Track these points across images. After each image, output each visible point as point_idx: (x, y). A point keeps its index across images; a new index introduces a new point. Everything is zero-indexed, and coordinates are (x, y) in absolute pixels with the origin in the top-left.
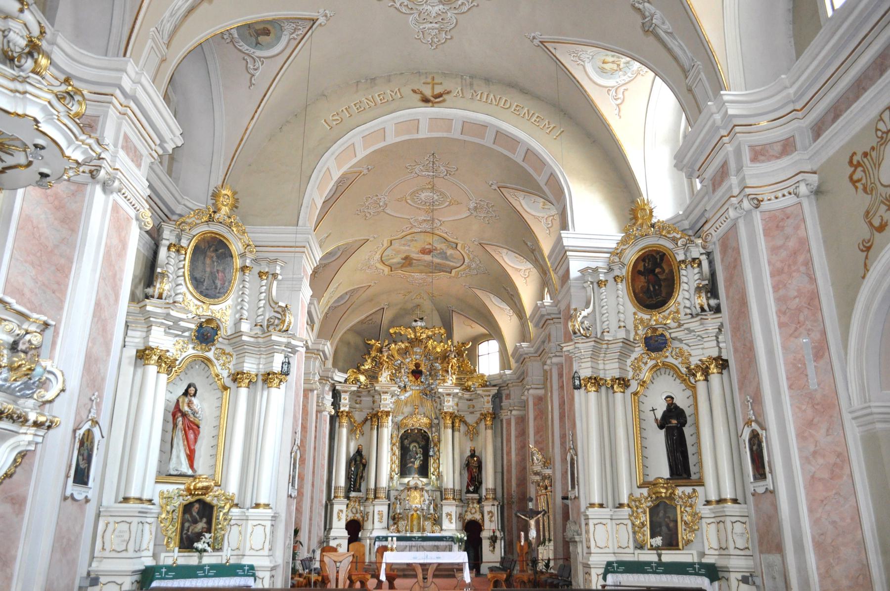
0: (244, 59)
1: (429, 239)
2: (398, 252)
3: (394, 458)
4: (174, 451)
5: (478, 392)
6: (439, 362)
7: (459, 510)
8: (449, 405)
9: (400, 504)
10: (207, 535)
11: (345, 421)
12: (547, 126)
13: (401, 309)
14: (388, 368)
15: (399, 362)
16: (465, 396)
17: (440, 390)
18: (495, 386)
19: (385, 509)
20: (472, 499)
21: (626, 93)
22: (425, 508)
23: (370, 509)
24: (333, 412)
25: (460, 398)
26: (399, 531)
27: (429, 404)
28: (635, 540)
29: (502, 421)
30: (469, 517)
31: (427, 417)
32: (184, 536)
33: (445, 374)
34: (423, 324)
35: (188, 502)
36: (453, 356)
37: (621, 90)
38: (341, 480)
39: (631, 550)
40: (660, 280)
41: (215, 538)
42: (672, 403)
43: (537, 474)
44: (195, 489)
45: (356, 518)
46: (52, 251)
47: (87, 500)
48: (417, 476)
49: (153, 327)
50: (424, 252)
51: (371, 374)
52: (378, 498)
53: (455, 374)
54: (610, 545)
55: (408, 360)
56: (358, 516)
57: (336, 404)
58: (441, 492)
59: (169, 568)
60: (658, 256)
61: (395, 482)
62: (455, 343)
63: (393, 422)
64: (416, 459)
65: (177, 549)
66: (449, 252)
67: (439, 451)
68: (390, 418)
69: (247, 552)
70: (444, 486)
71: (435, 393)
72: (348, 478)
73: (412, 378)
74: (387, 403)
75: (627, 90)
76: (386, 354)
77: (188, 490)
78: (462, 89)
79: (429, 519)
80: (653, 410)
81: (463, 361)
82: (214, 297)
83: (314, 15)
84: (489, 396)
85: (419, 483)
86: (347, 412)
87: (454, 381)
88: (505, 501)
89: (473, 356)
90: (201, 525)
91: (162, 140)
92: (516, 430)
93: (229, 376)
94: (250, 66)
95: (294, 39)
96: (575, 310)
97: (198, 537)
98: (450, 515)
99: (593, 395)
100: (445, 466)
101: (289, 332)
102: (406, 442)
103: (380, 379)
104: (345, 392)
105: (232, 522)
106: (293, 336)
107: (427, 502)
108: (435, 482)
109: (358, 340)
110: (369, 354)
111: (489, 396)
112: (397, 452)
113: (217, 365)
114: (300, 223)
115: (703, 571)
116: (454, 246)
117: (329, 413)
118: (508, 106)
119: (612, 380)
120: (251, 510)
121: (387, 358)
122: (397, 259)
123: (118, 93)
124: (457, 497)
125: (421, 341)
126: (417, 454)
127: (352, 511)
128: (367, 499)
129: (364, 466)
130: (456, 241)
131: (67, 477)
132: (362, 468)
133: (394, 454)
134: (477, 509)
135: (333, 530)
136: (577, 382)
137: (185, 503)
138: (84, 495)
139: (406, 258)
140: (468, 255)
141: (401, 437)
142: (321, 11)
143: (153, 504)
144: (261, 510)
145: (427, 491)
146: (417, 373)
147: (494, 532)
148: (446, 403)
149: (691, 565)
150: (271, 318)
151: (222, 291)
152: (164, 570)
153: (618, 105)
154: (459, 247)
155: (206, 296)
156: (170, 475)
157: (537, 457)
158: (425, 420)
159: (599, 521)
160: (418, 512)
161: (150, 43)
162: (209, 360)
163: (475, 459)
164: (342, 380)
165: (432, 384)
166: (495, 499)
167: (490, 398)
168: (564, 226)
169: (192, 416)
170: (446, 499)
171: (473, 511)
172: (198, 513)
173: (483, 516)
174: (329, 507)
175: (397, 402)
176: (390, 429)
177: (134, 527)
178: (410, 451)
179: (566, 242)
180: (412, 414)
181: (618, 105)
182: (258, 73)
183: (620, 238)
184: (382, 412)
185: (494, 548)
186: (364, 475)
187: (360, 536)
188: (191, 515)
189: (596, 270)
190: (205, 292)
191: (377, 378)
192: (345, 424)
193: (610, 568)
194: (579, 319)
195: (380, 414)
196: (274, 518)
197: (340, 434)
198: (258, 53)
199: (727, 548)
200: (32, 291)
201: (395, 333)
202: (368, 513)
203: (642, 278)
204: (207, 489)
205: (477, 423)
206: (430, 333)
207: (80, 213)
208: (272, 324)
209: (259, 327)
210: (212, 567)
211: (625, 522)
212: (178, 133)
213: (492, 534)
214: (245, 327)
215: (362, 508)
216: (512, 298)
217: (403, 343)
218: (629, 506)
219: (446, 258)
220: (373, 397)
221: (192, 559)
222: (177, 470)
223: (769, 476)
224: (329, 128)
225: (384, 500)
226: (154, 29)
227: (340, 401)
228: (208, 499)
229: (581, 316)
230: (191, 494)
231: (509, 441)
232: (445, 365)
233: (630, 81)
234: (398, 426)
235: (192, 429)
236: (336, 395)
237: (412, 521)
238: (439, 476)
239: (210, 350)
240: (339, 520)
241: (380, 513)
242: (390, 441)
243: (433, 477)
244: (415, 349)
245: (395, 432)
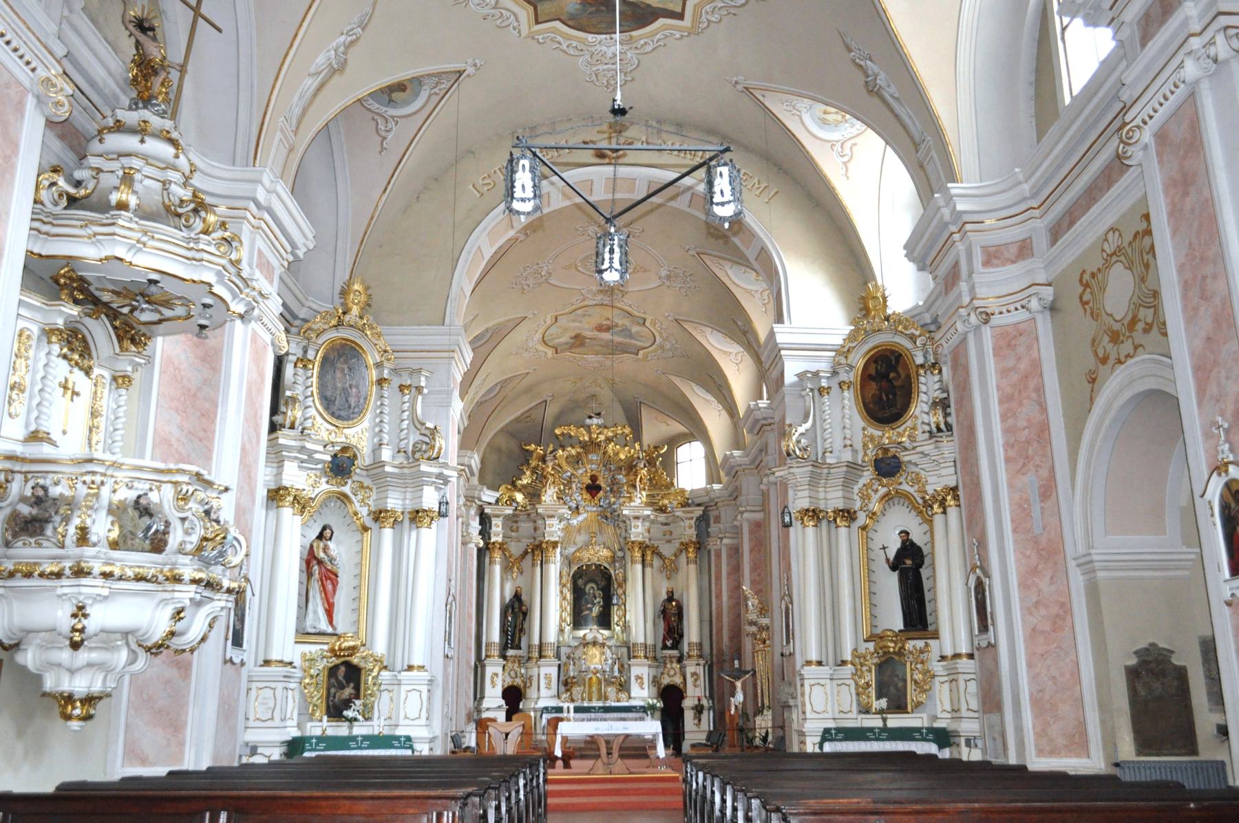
0: (373, 119)
1: (608, 313)
2: (566, 330)
3: (565, 604)
4: (310, 605)
5: (677, 514)
6: (624, 473)
7: (653, 671)
8: (638, 532)
9: (574, 664)
10: (358, 702)
11: (497, 556)
12: (756, 186)
13: (570, 400)
14: (554, 483)
15: (569, 474)
17: (625, 512)
18: (699, 505)
19: (553, 671)
20: (670, 657)
21: (854, 148)
23: (534, 672)
24: (481, 544)
25: (653, 522)
26: (573, 700)
27: (610, 530)
28: (859, 703)
29: (709, 552)
30: (666, 681)
31: (608, 548)
32: (331, 703)
33: (631, 490)
34: (600, 421)
36: (642, 466)
37: (848, 145)
38: (494, 633)
39: (854, 715)
40: (894, 387)
41: (365, 705)
42: (908, 539)
43: (752, 623)
44: (340, 649)
45: (515, 684)
46: (195, 395)
47: (242, 664)
48: (595, 627)
49: (286, 463)
50: (600, 328)
51: (531, 491)
52: (545, 657)
53: (644, 489)
54: (830, 712)
55: (580, 471)
56: (518, 681)
57: (485, 532)
58: (629, 648)
59: (320, 739)
60: (893, 358)
61: (566, 636)
62: (645, 448)
63: (561, 556)
64: (594, 604)
65: (325, 718)
66: (635, 329)
67: (625, 593)
68: (558, 550)
69: (402, 722)
70: (633, 640)
71: (618, 516)
72: (503, 631)
73: (587, 496)
74: (554, 530)
75: (856, 144)
76: (550, 464)
77: (332, 650)
79: (613, 683)
80: (884, 548)
81: (657, 471)
82: (348, 419)
83: (460, 66)
84: (692, 518)
87: (644, 499)
88: (714, 659)
89: (669, 464)
90: (348, 691)
91: (294, 246)
92: (728, 564)
93: (369, 515)
94: (381, 127)
95: (436, 94)
96: (790, 426)
97: (347, 704)
98: (641, 678)
99: (810, 531)
100: (633, 613)
101: (441, 460)
102: (580, 582)
103: (543, 498)
104: (497, 516)
105: (383, 687)
106: (445, 465)
107: (610, 662)
108: (621, 636)
109: (513, 445)
110: (529, 464)
111: (692, 518)
112: (569, 596)
113: (355, 501)
114: (447, 321)
115: (931, 736)
116: (642, 322)
117: (476, 545)
119: (834, 512)
120: (403, 673)
121: (553, 468)
122: (565, 339)
123: (252, 206)
124: (651, 655)
125: (598, 445)
128: (529, 659)
129: (525, 614)
131: (226, 639)
133: (564, 599)
134: (678, 671)
136: (787, 519)
137: (330, 665)
138: (241, 658)
139: (577, 337)
140: (660, 333)
141: (574, 576)
142: (470, 61)
143: (295, 667)
144: (415, 673)
145: (610, 647)
146: (593, 489)
147: (699, 700)
149: (918, 730)
150: (417, 443)
151: (356, 410)
152: (314, 741)
153: (845, 163)
154: (648, 324)
155: (339, 417)
156: (308, 634)
158: (605, 553)
159: (817, 681)
160: (598, 675)
161: (279, 135)
162: (345, 496)
163: (674, 603)
164: (493, 501)
165: (614, 503)
166: (700, 656)
167: (693, 522)
168: (779, 319)
170: (634, 657)
171: (672, 673)
173: (685, 679)
174: (479, 669)
175: (567, 529)
176: (558, 564)
177: (279, 692)
178: (585, 593)
179: (780, 339)
180: (587, 545)
181: (845, 163)
182: (390, 136)
183: (847, 332)
184: (547, 542)
185: (700, 720)
186: (526, 626)
188: (337, 679)
189: (816, 374)
190: (337, 413)
191: (539, 496)
192: (498, 560)
193: (827, 735)
194: (794, 438)
195: (544, 546)
196: (431, 682)
197: (491, 572)
198: (392, 112)
199: (959, 710)
200: (178, 440)
201: (563, 434)
202: (531, 677)
203: (874, 384)
204: (353, 649)
205: (676, 555)
206: (610, 434)
207: (221, 350)
208: (420, 451)
209: (402, 454)
210: (365, 738)
211: (847, 682)
212: (310, 236)
213: (697, 702)
214: (386, 454)
215: (523, 671)
216: (719, 388)
217: (573, 448)
218: (852, 664)
219: (631, 336)
220: (535, 522)
221: (341, 730)
223: (991, 628)
224: (478, 195)
225: (553, 659)
226: (283, 118)
227: (490, 528)
228: (355, 660)
229: (797, 434)
231: (719, 578)
233: (858, 135)
234: (568, 561)
235: (330, 579)
236: (485, 520)
237: (590, 686)
238: (626, 627)
239: (346, 483)
240: (494, 687)
241: (548, 677)
244: (590, 456)
245: (566, 570)
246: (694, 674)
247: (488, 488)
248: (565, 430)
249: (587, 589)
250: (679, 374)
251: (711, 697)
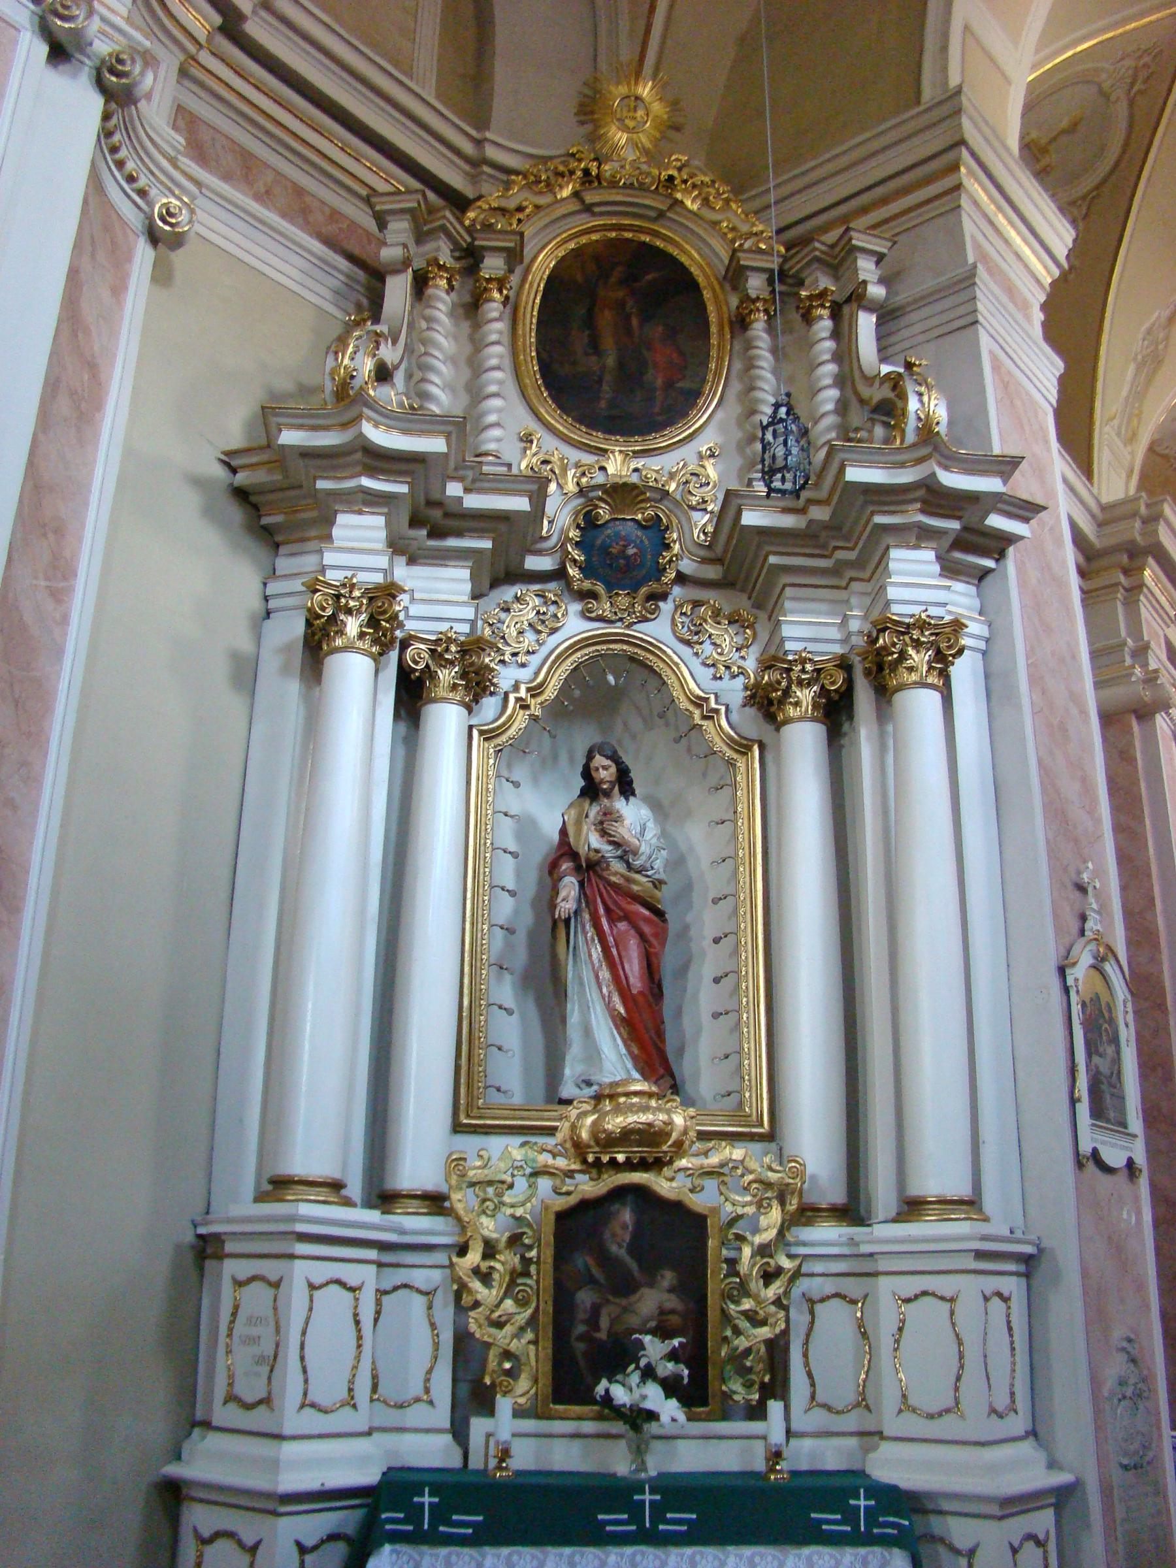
35: (572, 1200)
172: (633, 1249)
222: (589, 1083)
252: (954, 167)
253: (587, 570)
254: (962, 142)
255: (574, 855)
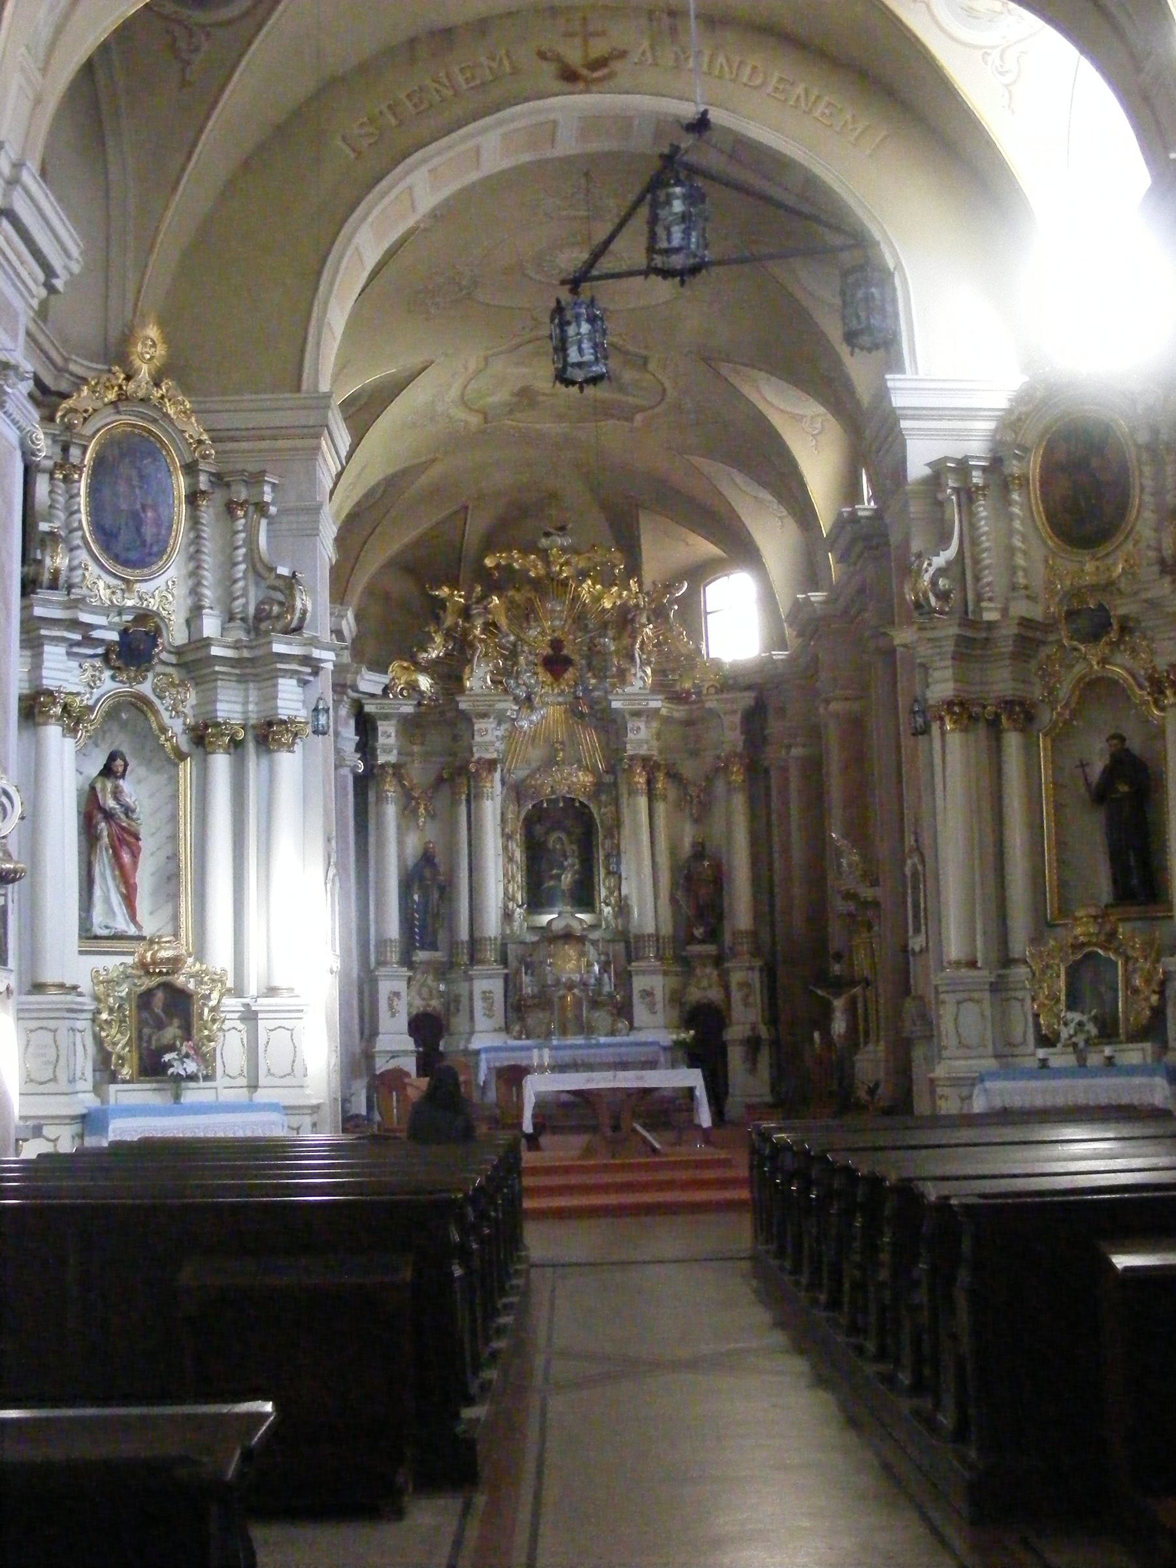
5: (708, 705)
7: (673, 982)
11: (391, 789)
14: (486, 655)
15: (512, 638)
16: (676, 715)
17: (616, 705)
19: (496, 987)
20: (700, 956)
22: (592, 981)
23: (462, 988)
25: (667, 720)
30: (695, 995)
31: (587, 769)
33: (624, 664)
34: (566, 541)
36: (644, 620)
43: (850, 896)
48: (569, 908)
52: (481, 962)
53: (649, 663)
55: (533, 633)
57: (366, 747)
58: (627, 943)
61: (516, 924)
62: (648, 586)
63: (503, 782)
64: (562, 868)
68: (497, 776)
70: (634, 929)
73: (544, 676)
76: (479, 623)
78: (652, 47)
84: (734, 712)
85: (576, 926)
86: (394, 766)
102: (539, 829)
103: (468, 684)
104: (386, 717)
110: (438, 620)
111: (734, 712)
112: (518, 855)
118: (758, 81)
124: (669, 953)
125: (564, 583)
126: (566, 857)
127: (420, 994)
130: (644, 352)
132: (436, 896)
133: (511, 860)
135: (380, 1036)
141: (526, 819)
145: (594, 943)
146: (556, 663)
148: (630, 735)
154: (652, 366)
157: (850, 859)
160: (576, 991)
163: (706, 863)
167: (737, 718)
169: (123, 816)
170: (637, 959)
175: (509, 737)
176: (498, 800)
187: (441, 1048)
191: (459, 679)
195: (472, 768)
197: (380, 816)
201: (498, 566)
205: (709, 779)
215: (442, 987)
217: (518, 590)
222: (107, 927)
225: (495, 966)
227: (375, 738)
230: (148, 973)
232: (626, 641)
234: (517, 792)
236: (365, 725)
237: (563, 1008)
238: (622, 909)
240: (393, 1015)
241: (487, 996)
242: (499, 829)
243: (607, 910)
244: (549, 606)
246: (744, 985)
247: (370, 669)
248: (502, 558)
249: (550, 845)
250: (709, 453)
251: (773, 1020)
252: (318, 436)
253: (119, 655)
254: (327, 426)
255: (102, 810)
